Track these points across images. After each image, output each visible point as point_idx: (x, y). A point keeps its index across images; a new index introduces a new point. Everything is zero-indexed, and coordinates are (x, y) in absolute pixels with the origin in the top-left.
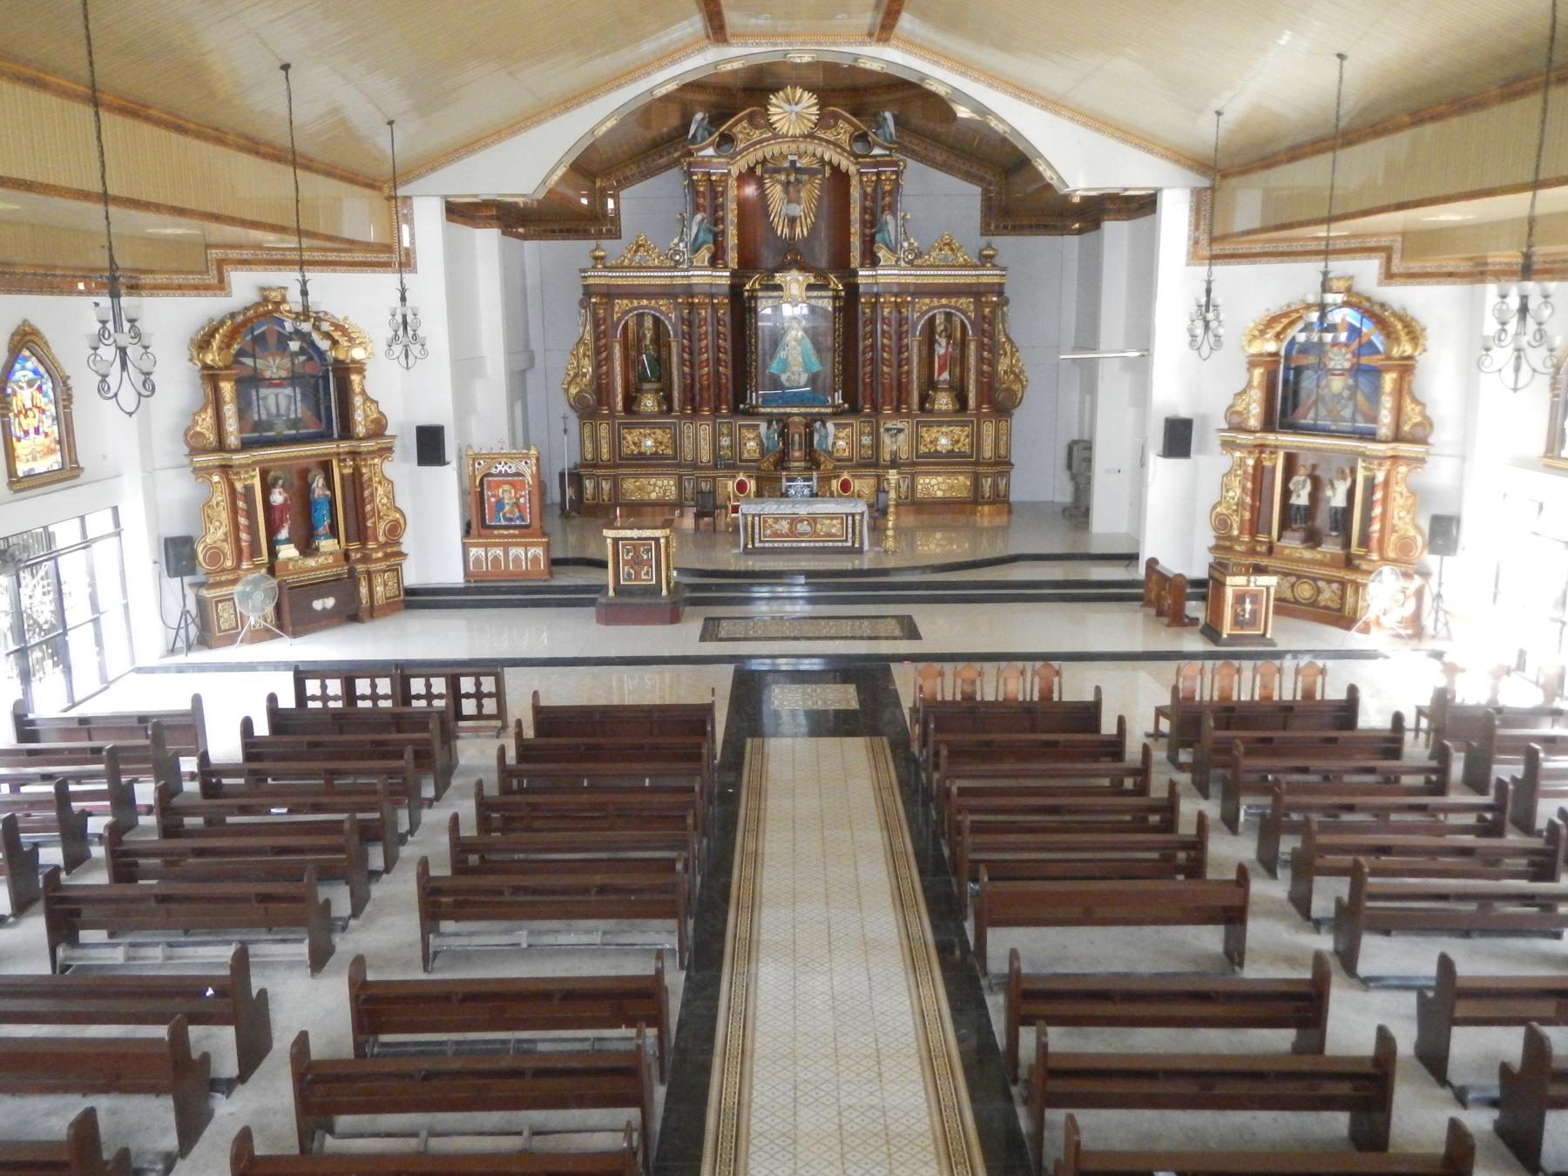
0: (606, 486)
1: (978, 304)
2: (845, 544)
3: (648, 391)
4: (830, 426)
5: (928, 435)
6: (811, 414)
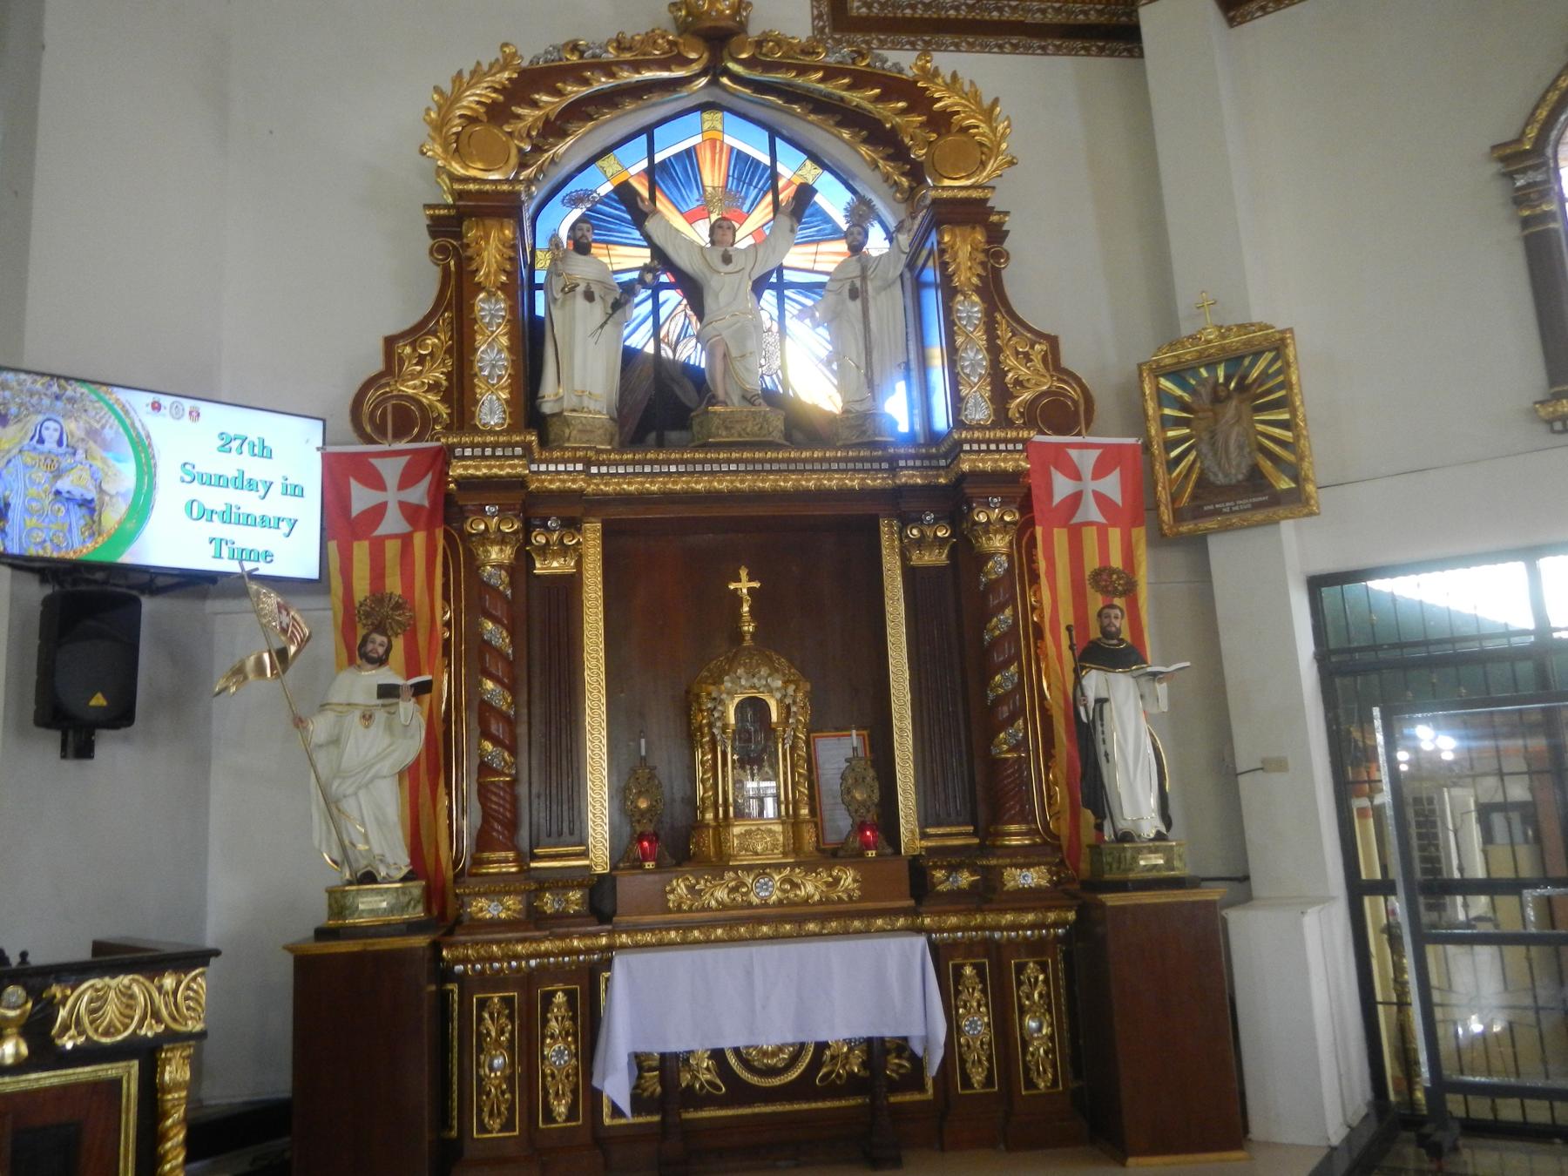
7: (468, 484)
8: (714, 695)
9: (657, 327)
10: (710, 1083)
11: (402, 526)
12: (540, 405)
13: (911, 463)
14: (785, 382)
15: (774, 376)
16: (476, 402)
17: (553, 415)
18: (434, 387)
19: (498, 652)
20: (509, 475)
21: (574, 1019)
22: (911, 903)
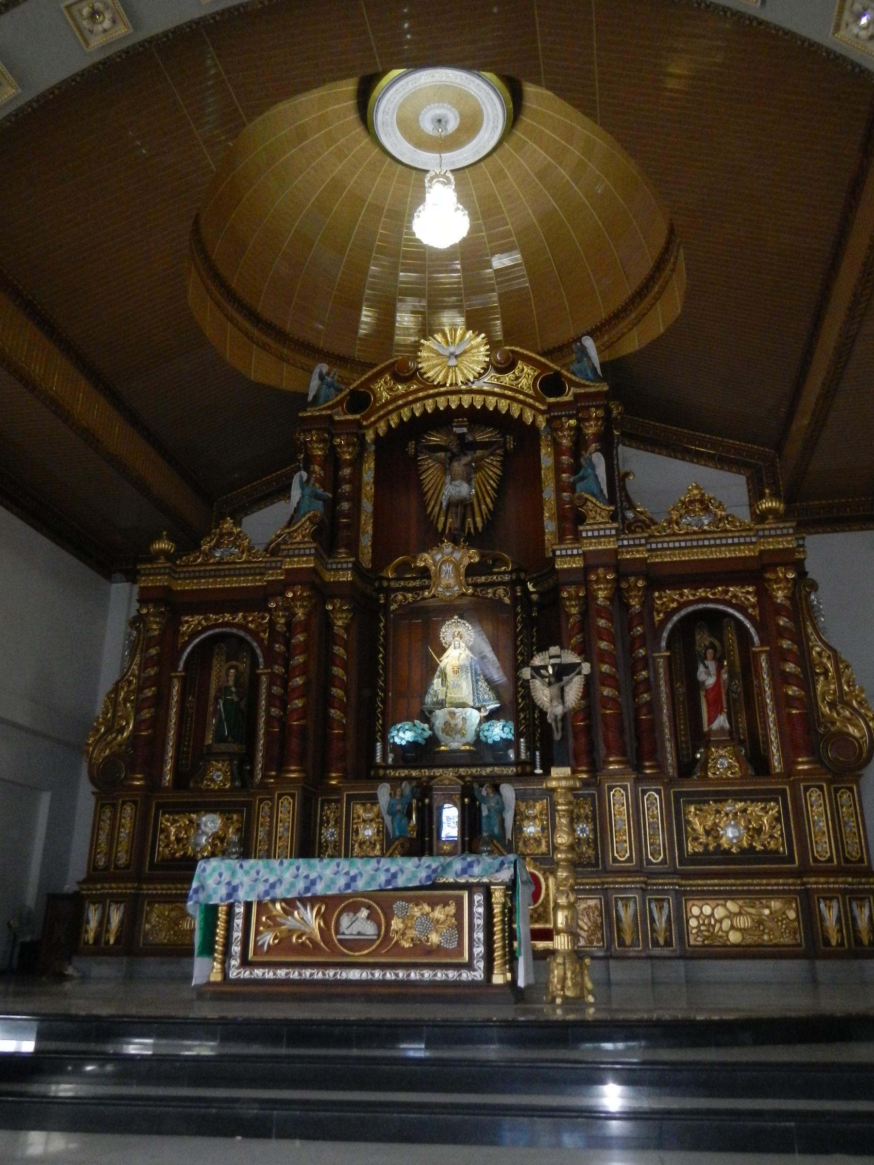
0: (116, 918)
1: (763, 594)
2: (466, 976)
3: (218, 756)
4: (508, 791)
6: (473, 777)
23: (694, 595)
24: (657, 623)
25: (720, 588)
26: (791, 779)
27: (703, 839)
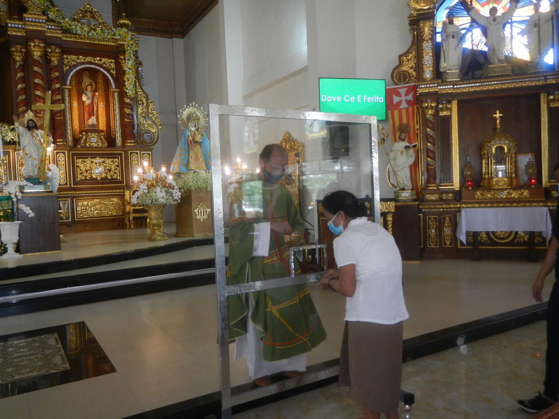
5: (82, 165)
7: (422, 94)
8: (489, 145)
9: (472, 41)
10: (486, 241)
11: (406, 106)
12: (440, 69)
13: (551, 77)
14: (512, 53)
15: (509, 51)
16: (424, 72)
17: (443, 72)
18: (412, 68)
19: (431, 137)
20: (433, 91)
21: (451, 223)
22: (544, 199)
23: (84, 60)
24: (65, 71)
25: (98, 58)
26: (125, 149)
27: (85, 174)
